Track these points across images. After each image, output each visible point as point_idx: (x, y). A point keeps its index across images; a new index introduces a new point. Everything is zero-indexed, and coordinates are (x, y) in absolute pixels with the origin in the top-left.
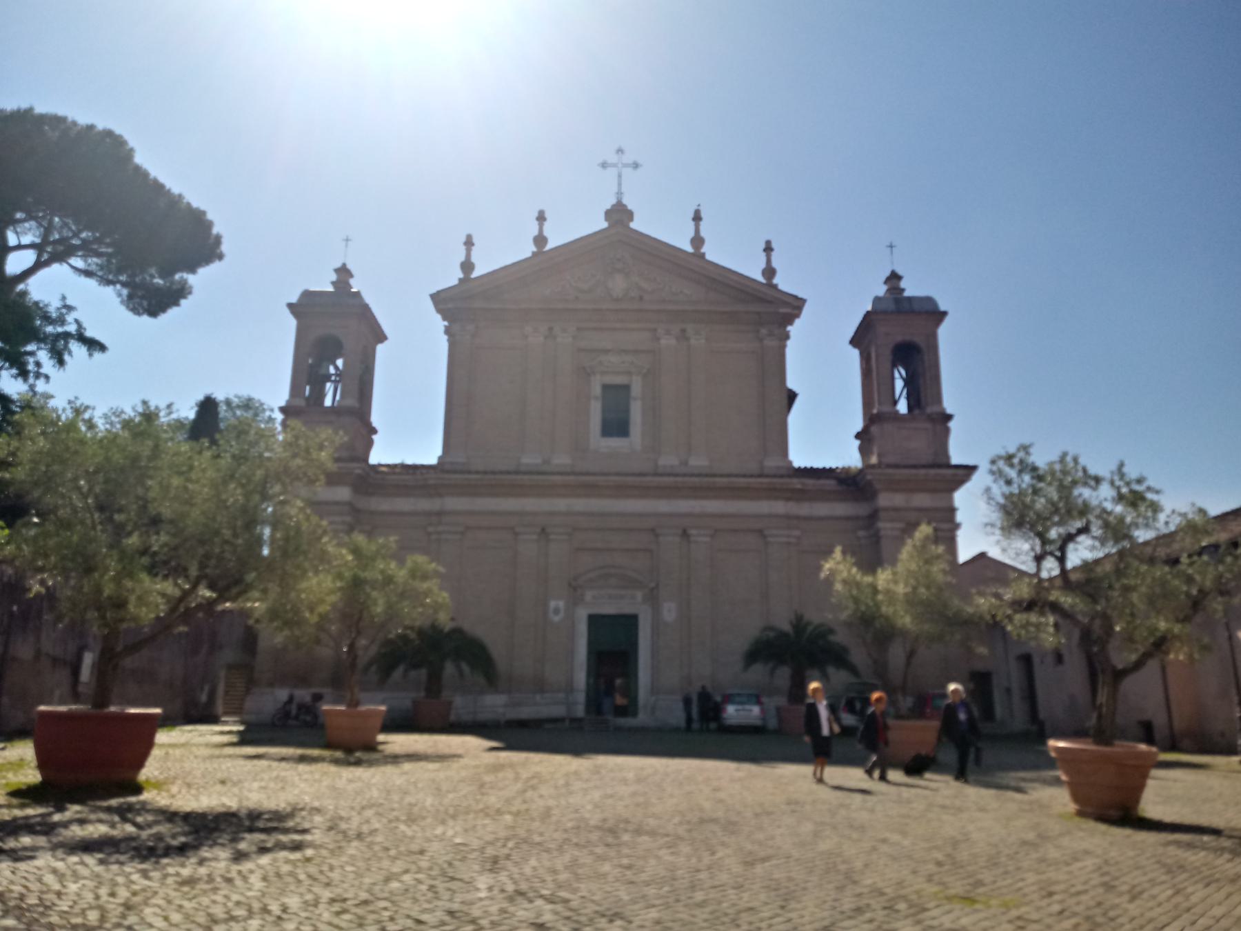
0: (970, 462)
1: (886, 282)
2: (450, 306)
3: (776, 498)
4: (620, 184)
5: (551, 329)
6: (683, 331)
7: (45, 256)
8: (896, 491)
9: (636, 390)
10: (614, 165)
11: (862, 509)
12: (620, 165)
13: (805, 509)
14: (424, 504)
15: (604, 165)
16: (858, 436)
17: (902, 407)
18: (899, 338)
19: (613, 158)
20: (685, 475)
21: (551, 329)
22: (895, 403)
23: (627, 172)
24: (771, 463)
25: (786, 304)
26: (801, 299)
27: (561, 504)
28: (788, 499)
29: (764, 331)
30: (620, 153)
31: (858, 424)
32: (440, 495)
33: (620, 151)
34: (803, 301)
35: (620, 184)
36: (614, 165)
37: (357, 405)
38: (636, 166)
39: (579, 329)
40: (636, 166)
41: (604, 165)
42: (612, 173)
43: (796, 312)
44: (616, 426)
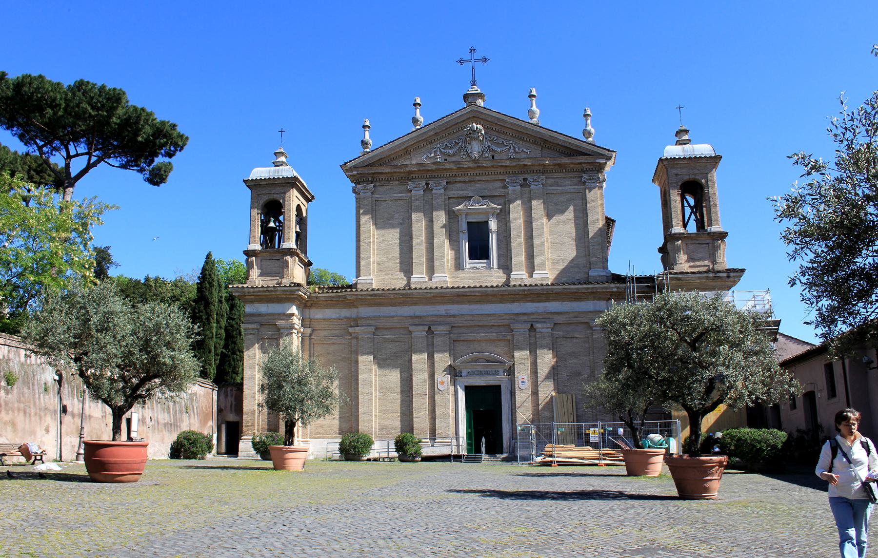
1: (676, 135)
2: (355, 173)
3: (599, 299)
4: (473, 75)
5: (427, 184)
6: (525, 180)
7: (93, 159)
9: (493, 225)
10: (469, 61)
12: (473, 61)
14: (345, 313)
15: (461, 62)
17: (692, 228)
18: (686, 178)
19: (467, 56)
21: (427, 184)
22: (685, 225)
23: (479, 65)
25: (602, 156)
33: (472, 50)
35: (473, 75)
36: (469, 61)
39: (447, 183)
40: (485, 60)
41: (461, 62)
44: (479, 251)
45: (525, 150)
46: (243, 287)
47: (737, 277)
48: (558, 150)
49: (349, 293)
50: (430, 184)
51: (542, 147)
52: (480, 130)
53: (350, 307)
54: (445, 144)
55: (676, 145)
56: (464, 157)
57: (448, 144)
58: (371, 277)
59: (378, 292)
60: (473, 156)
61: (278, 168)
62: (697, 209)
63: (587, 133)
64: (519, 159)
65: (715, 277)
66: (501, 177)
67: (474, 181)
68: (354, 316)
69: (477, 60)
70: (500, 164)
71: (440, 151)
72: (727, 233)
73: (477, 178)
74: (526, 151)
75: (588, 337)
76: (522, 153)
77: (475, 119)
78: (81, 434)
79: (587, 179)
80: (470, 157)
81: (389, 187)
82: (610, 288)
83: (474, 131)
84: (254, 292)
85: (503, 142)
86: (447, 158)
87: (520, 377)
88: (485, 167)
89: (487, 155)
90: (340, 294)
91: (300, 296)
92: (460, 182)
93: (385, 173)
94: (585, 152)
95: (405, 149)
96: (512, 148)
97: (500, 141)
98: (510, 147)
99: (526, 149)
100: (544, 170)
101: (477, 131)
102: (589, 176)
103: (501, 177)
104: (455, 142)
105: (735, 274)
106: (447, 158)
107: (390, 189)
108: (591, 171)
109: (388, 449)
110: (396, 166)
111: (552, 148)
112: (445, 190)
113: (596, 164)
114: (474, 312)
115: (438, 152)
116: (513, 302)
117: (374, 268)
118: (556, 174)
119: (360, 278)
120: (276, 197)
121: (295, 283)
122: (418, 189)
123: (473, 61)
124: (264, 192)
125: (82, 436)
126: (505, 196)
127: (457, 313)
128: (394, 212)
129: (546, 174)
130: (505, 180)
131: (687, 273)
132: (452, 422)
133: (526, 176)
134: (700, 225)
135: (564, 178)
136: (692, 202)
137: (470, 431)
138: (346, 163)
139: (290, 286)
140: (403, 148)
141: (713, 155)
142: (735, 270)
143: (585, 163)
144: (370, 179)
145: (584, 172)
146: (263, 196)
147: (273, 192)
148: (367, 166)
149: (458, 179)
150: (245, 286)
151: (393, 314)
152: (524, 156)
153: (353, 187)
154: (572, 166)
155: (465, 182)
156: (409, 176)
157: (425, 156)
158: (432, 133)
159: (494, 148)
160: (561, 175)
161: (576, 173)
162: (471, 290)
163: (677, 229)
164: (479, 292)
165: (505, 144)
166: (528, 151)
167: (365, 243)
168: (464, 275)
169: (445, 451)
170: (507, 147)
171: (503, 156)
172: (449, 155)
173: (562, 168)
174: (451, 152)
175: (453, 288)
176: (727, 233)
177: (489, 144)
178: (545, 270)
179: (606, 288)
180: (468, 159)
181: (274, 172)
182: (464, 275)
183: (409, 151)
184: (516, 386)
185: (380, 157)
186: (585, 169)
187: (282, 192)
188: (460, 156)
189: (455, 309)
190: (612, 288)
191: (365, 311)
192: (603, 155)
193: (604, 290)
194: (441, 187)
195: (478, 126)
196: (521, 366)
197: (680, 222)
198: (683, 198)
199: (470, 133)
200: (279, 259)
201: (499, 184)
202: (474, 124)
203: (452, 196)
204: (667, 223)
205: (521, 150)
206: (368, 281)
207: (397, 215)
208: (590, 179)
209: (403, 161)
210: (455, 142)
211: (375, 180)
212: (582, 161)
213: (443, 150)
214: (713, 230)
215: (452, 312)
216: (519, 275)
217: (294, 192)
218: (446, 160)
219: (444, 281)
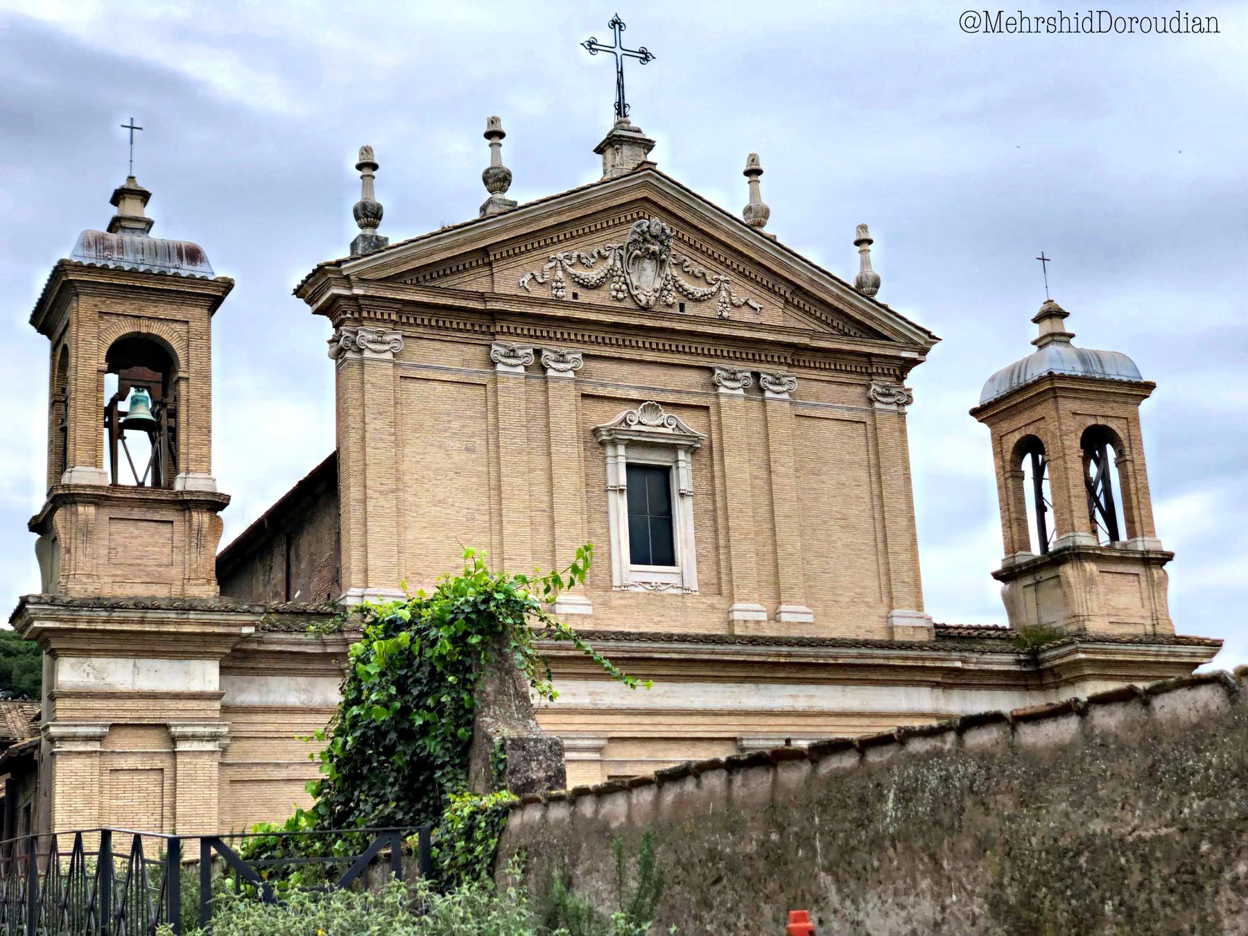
0: (1213, 636)
2: (358, 291)
4: (620, 86)
5: (538, 353)
20: (777, 641)
21: (538, 353)
23: (631, 65)
24: (906, 623)
25: (912, 345)
35: (620, 86)
38: (645, 56)
45: (751, 302)
51: (787, 301)
54: (575, 254)
57: (583, 255)
60: (642, 297)
69: (629, 53)
71: (564, 270)
73: (649, 356)
74: (755, 305)
76: (745, 309)
77: (647, 205)
79: (878, 394)
81: (437, 345)
83: (655, 237)
85: (704, 274)
89: (670, 300)
94: (879, 329)
96: (724, 293)
97: (697, 269)
98: (719, 289)
103: (703, 362)
104: (599, 253)
106: (578, 290)
113: (897, 362)
115: (560, 274)
118: (815, 372)
119: (369, 591)
120: (156, 329)
126: (707, 408)
128: (449, 415)
144: (394, 317)
146: (114, 319)
152: (747, 316)
157: (529, 277)
159: (689, 286)
160: (824, 375)
167: (381, 492)
168: (624, 602)
170: (714, 289)
171: (705, 310)
172: (586, 286)
174: (593, 275)
180: (628, 304)
182: (624, 602)
183: (492, 258)
192: (916, 343)
199: (645, 240)
207: (456, 425)
208: (884, 395)
209: (476, 282)
210: (599, 253)
212: (876, 351)
213: (571, 270)
218: (575, 296)
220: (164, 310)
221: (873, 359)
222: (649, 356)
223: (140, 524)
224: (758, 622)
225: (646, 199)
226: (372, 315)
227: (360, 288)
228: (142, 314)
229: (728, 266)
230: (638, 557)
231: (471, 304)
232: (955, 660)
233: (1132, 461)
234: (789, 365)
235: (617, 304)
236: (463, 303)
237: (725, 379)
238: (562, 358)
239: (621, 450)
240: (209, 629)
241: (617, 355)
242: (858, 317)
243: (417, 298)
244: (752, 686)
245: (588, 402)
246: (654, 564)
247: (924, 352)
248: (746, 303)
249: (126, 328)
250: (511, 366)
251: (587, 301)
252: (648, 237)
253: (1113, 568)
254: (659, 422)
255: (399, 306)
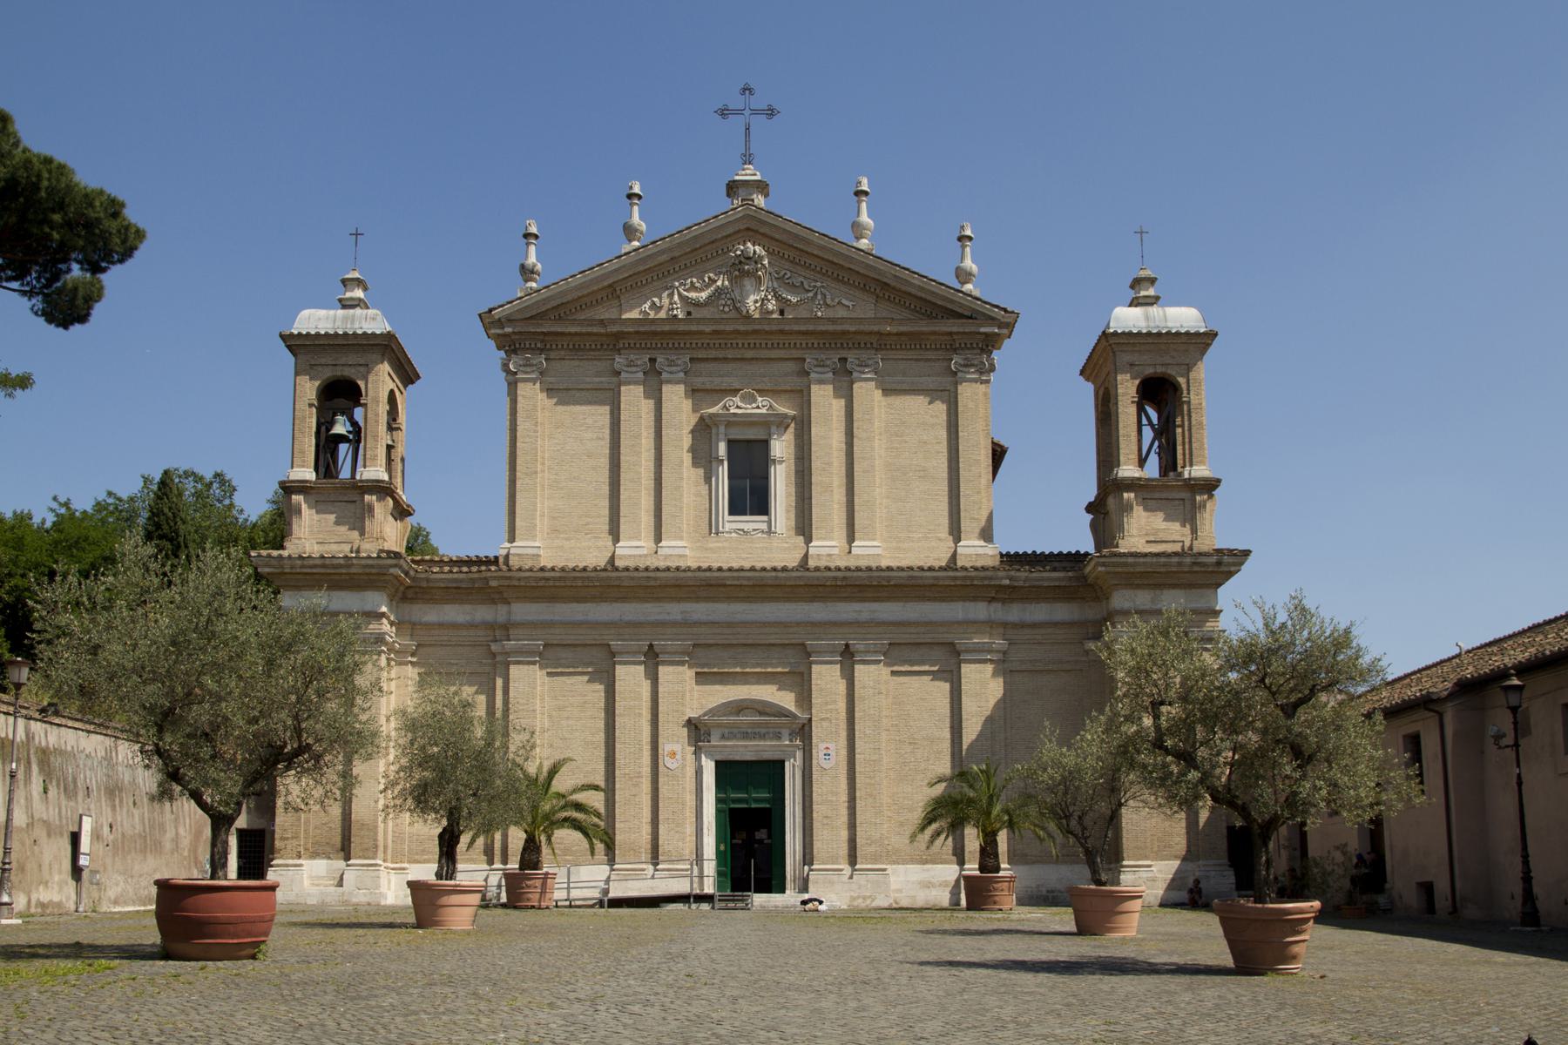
1: (1132, 287)
2: (508, 330)
3: (975, 599)
5: (652, 360)
6: (844, 360)
8: (1138, 587)
10: (739, 112)
11: (1091, 612)
12: (747, 112)
13: (1015, 613)
14: (483, 613)
15: (724, 112)
16: (1090, 508)
18: (1149, 371)
19: (737, 102)
21: (652, 360)
22: (1142, 462)
23: (758, 122)
25: (992, 320)
26: (1013, 312)
27: (674, 611)
28: (992, 600)
29: (956, 359)
30: (747, 92)
31: (1091, 493)
32: (507, 602)
33: (747, 90)
34: (1006, 322)
36: (739, 112)
37: (386, 478)
40: (771, 112)
41: (724, 112)
42: (737, 123)
43: (1005, 331)
45: (844, 301)
46: (280, 556)
47: (1234, 564)
48: (907, 304)
49: (495, 574)
50: (658, 360)
52: (761, 258)
53: (493, 602)
55: (1130, 306)
56: (727, 309)
58: (537, 544)
59: (552, 574)
61: (351, 311)
62: (1165, 433)
63: (963, 276)
64: (833, 321)
65: (1194, 563)
66: (796, 354)
67: (742, 359)
68: (501, 618)
69: (755, 112)
70: (796, 328)
72: (1219, 481)
73: (749, 354)
75: (951, 671)
76: (838, 307)
77: (751, 233)
78: (4, 864)
79: (961, 365)
80: (737, 309)
81: (576, 363)
82: (997, 578)
83: (749, 258)
84: (303, 566)
85: (802, 283)
86: (691, 309)
87: (822, 746)
88: (767, 332)
90: (476, 576)
91: (397, 577)
92: (715, 359)
93: (570, 334)
94: (960, 310)
95: (610, 286)
96: (819, 297)
97: (797, 280)
98: (816, 294)
99: (847, 299)
100: (877, 342)
101: (756, 260)
102: (965, 359)
103: (796, 354)
104: (709, 278)
105: (1231, 560)
106: (691, 309)
107: (578, 366)
108: (968, 349)
109: (569, 883)
110: (591, 322)
111: (897, 301)
112: (686, 373)
113: (979, 336)
114: (739, 617)
116: (813, 599)
117: (542, 524)
118: (900, 352)
119: (515, 544)
120: (348, 372)
121: (389, 552)
122: (634, 369)
123: (747, 112)
124: (323, 361)
125: (7, 866)
127: (704, 618)
129: (883, 352)
130: (804, 360)
131: (1146, 555)
132: (690, 829)
133: (844, 354)
134: (1169, 464)
135: (917, 360)
136: (1154, 415)
137: (722, 847)
138: (490, 311)
139: (379, 557)
140: (606, 283)
141: (1202, 331)
142: (1231, 552)
143: (958, 333)
144: (539, 345)
145: (955, 350)
146: (320, 369)
147: (343, 361)
148: (532, 318)
149: (713, 354)
150: (285, 553)
151: (580, 617)
152: (841, 313)
153: (502, 359)
154: (933, 337)
155: (725, 359)
156: (617, 340)
157: (649, 303)
158: (665, 257)
160: (911, 355)
161: (940, 353)
162: (735, 574)
163: (1128, 470)
164: (749, 578)
165: (807, 287)
166: (850, 304)
167: (526, 474)
168: (720, 545)
169: (681, 887)
170: (811, 294)
172: (697, 304)
173: (912, 341)
175: (699, 569)
176: (1219, 481)
177: (776, 285)
178: (874, 540)
179: (991, 578)
180: (733, 314)
181: (345, 319)
182: (720, 545)
183: (618, 292)
184: (814, 762)
185: (559, 301)
186: (958, 345)
187: (362, 362)
188: (718, 306)
189: (700, 611)
190: (1002, 578)
191: (523, 611)
192: (993, 319)
193: (986, 583)
194: (679, 368)
195: (757, 248)
196: (825, 724)
197: (1134, 457)
198: (1141, 410)
199: (740, 262)
200: (355, 502)
201: (791, 366)
202: (749, 245)
203: (699, 386)
204: (1107, 456)
205: (837, 300)
206: (530, 551)
209: (605, 313)
210: (709, 278)
211: (548, 346)
212: (955, 329)
214: (1194, 474)
215: (695, 617)
216: (828, 548)
217: (385, 368)
218: (689, 313)
219: (680, 556)
220: (352, 358)
221: (955, 337)
222: (749, 354)
223: (336, 504)
224: (830, 555)
225: (748, 229)
226: (522, 346)
227: (509, 327)
228: (338, 362)
229: (824, 274)
230: (736, 509)
231: (595, 330)
232: (1002, 578)
233: (1189, 403)
234: (877, 349)
235: (724, 316)
236: (590, 329)
237: (816, 366)
238: (671, 363)
239: (722, 429)
240: (367, 571)
241: (739, 356)
242: (939, 303)
243: (552, 329)
244: (821, 604)
245: (697, 394)
246: (751, 514)
247: (1010, 326)
248: (839, 303)
249: (328, 373)
250: (632, 372)
251: (698, 316)
252: (743, 260)
253: (1157, 495)
254: (754, 405)
255: (542, 337)
